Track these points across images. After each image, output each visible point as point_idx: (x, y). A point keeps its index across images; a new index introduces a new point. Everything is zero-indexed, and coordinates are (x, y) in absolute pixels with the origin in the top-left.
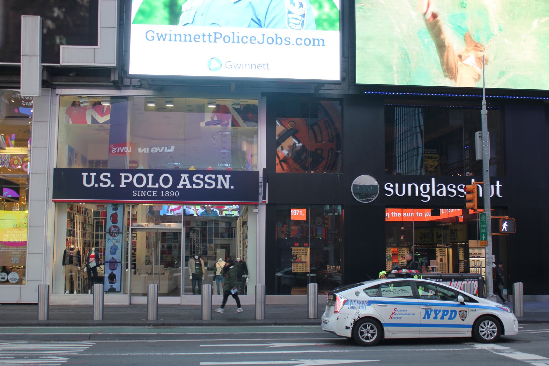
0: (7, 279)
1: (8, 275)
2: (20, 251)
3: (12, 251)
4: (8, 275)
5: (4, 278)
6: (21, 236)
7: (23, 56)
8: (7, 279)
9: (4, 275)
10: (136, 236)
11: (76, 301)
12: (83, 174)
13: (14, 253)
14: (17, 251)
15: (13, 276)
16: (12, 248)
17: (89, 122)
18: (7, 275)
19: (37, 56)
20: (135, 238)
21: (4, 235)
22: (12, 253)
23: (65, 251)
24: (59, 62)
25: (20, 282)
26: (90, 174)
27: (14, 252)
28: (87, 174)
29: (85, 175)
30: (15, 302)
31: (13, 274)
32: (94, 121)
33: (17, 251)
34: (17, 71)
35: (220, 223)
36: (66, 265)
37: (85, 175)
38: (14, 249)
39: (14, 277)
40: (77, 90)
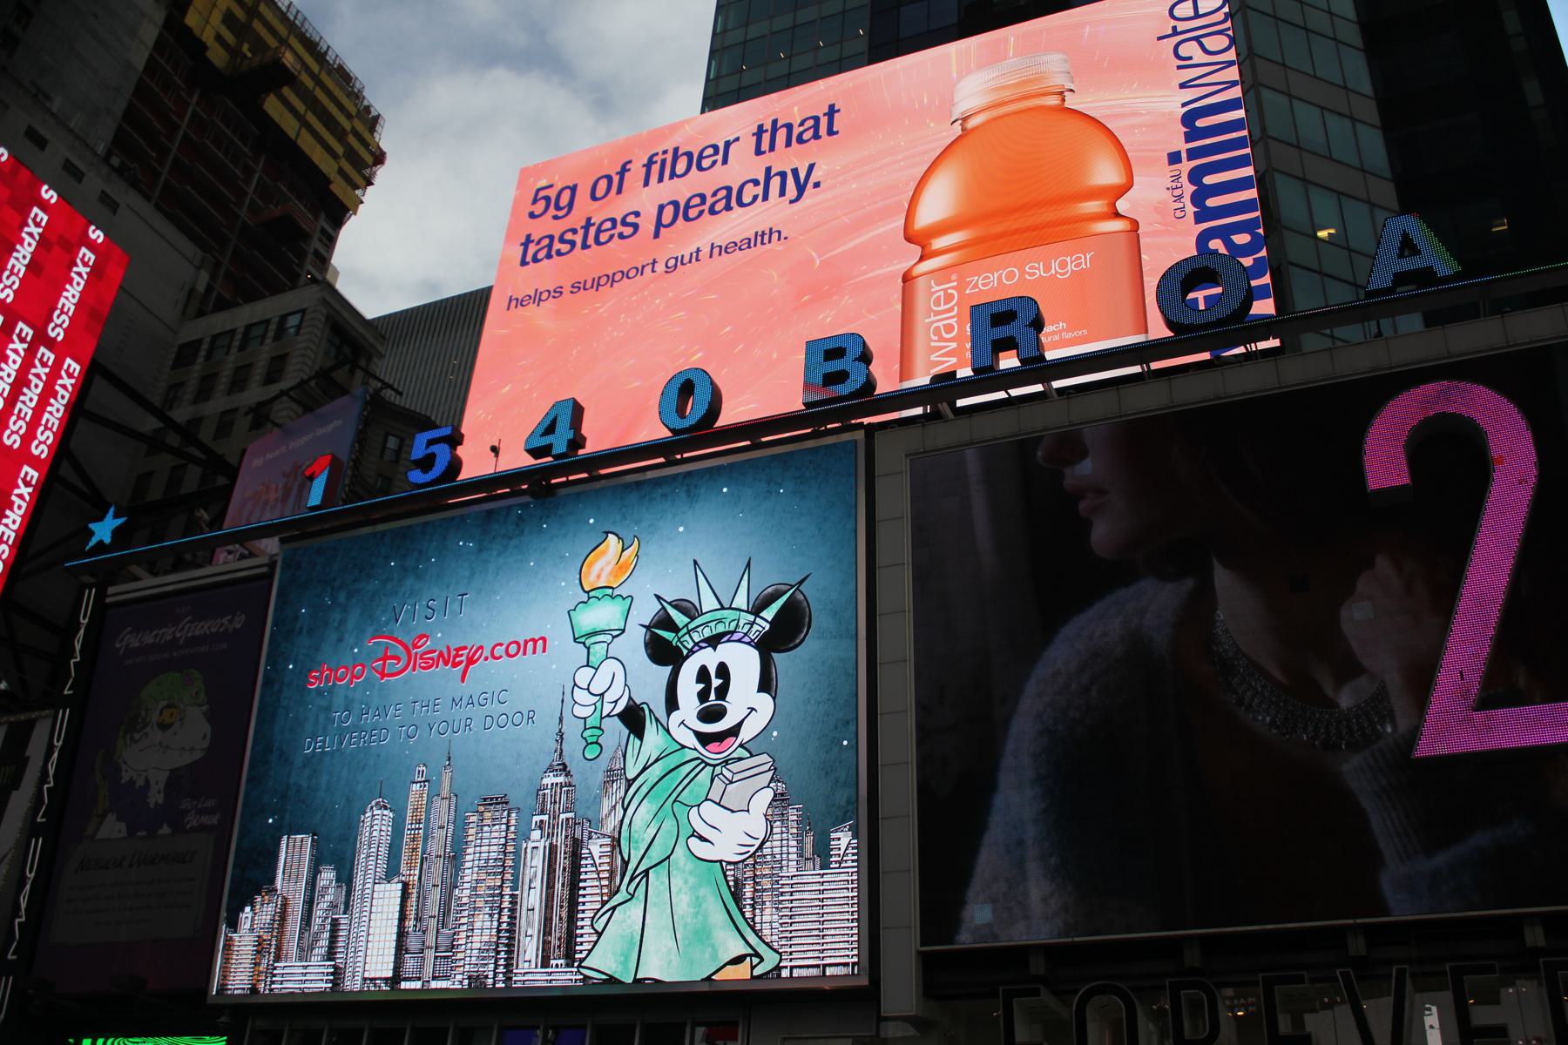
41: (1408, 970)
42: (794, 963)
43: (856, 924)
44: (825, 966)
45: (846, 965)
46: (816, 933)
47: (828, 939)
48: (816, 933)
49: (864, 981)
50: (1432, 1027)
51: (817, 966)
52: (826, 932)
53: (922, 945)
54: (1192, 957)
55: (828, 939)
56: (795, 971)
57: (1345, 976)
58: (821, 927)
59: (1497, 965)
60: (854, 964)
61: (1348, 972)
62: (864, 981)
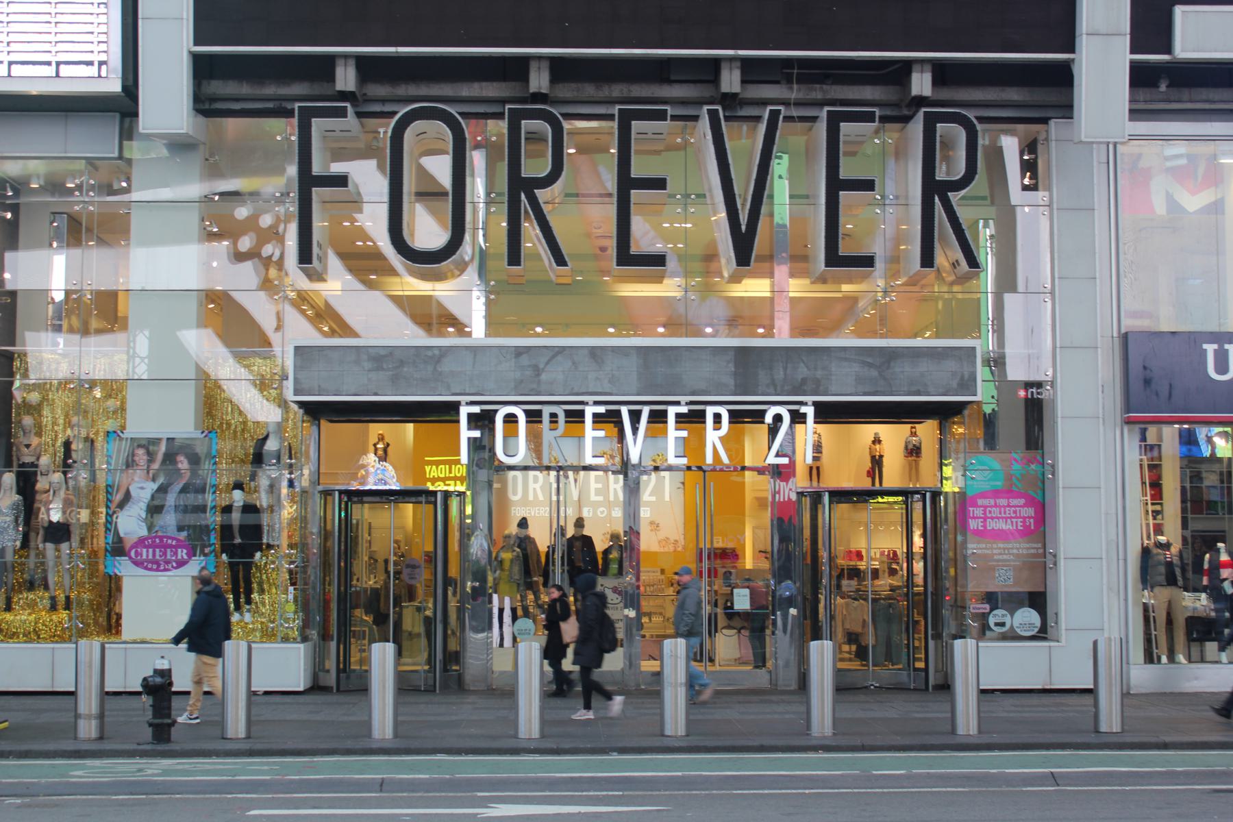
0: (1012, 626)
1: (1012, 616)
2: (1015, 551)
3: (995, 551)
4: (1012, 616)
5: (1003, 624)
6: (1015, 512)
7: (1087, 34)
8: (1012, 626)
9: (1003, 616)
10: (1162, 510)
11: (1195, 682)
12: (1205, 346)
13: (1000, 557)
14: (1006, 552)
15: (1025, 619)
16: (995, 546)
17: (1160, 208)
18: (1009, 616)
19: (1126, 35)
20: (1159, 517)
21: (971, 509)
22: (995, 557)
23: (1146, 552)
24: (1168, 49)
25: (1042, 634)
26: (1223, 346)
27: (1001, 554)
28: (1215, 346)
29: (1210, 348)
30: (1040, 687)
31: (1026, 614)
32: (1173, 205)
33: (1006, 552)
34: (1062, 77)
35: (1204, 475)
36: (1152, 588)
37: (1210, 348)
38: (1000, 548)
39: (1027, 620)
40: (1209, 124)
41: (782, 112)
42: (13, 57)
43: (105, 11)
44: (58, 64)
45: (90, 63)
46: (47, 18)
47: (61, 28)
48: (47, 18)
49: (114, 86)
50: (780, 177)
51: (49, 63)
52: (60, 18)
53: (196, 44)
54: (539, 81)
55: (61, 28)
56: (13, 67)
57: (713, 115)
58: (53, 11)
59: (877, 114)
60: (101, 63)
61: (718, 110)
62: (114, 86)
